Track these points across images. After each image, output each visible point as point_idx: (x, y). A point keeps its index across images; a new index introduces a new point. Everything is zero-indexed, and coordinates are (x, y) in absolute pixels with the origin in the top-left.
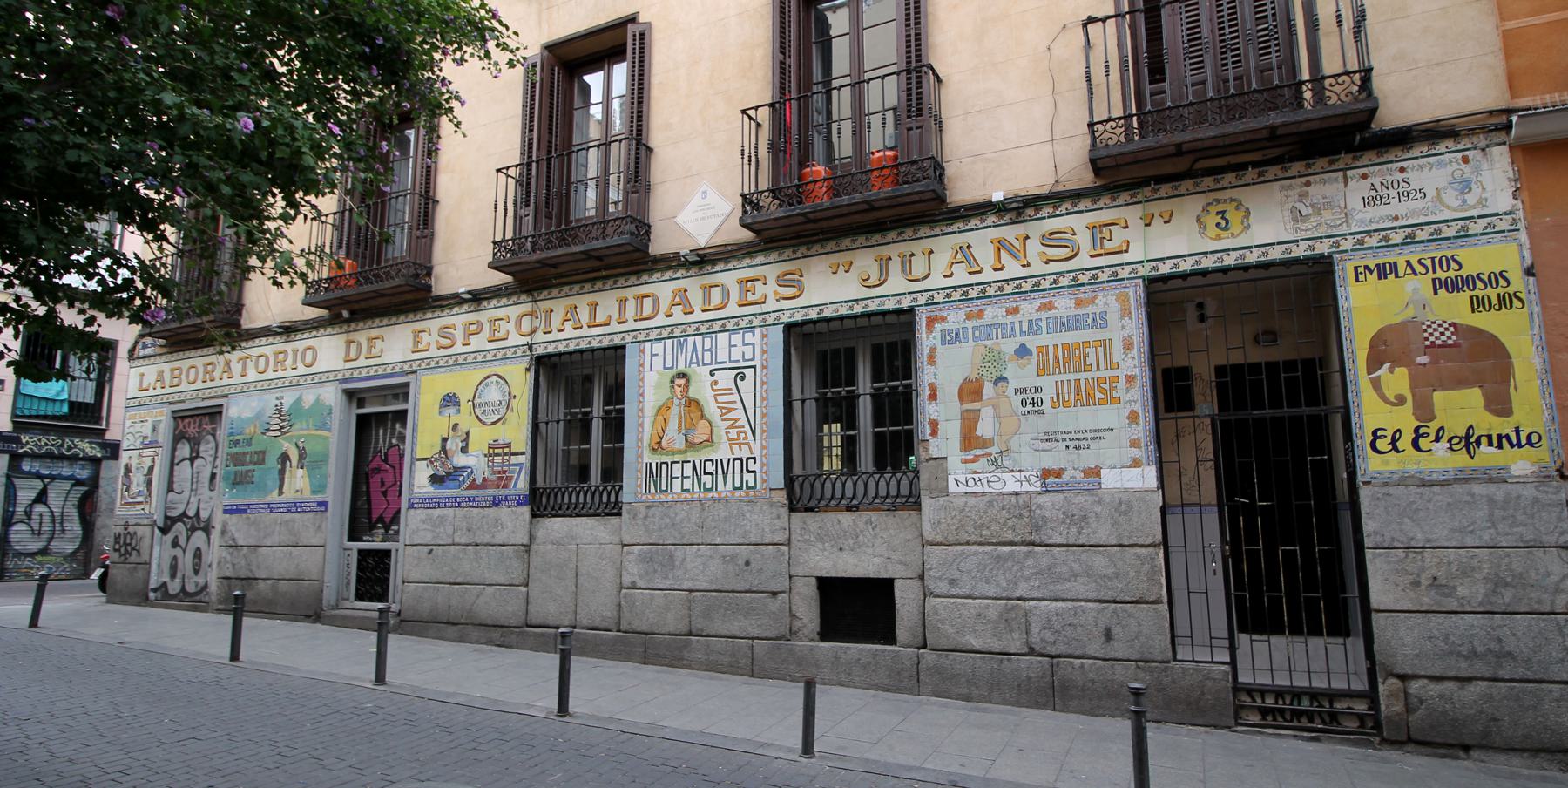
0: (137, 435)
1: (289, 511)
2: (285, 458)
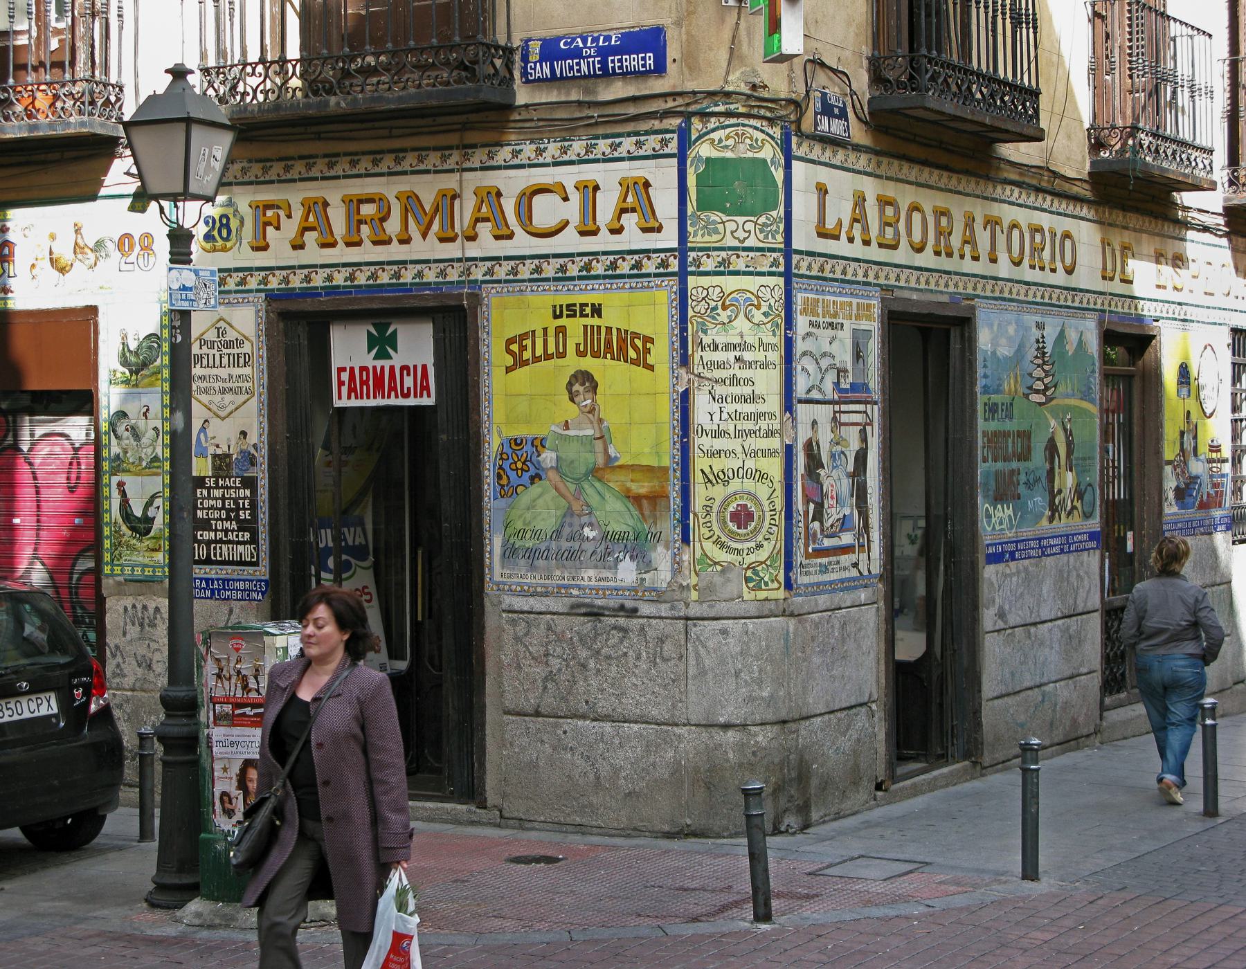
0: (825, 363)
1: (1062, 551)
2: (1052, 448)
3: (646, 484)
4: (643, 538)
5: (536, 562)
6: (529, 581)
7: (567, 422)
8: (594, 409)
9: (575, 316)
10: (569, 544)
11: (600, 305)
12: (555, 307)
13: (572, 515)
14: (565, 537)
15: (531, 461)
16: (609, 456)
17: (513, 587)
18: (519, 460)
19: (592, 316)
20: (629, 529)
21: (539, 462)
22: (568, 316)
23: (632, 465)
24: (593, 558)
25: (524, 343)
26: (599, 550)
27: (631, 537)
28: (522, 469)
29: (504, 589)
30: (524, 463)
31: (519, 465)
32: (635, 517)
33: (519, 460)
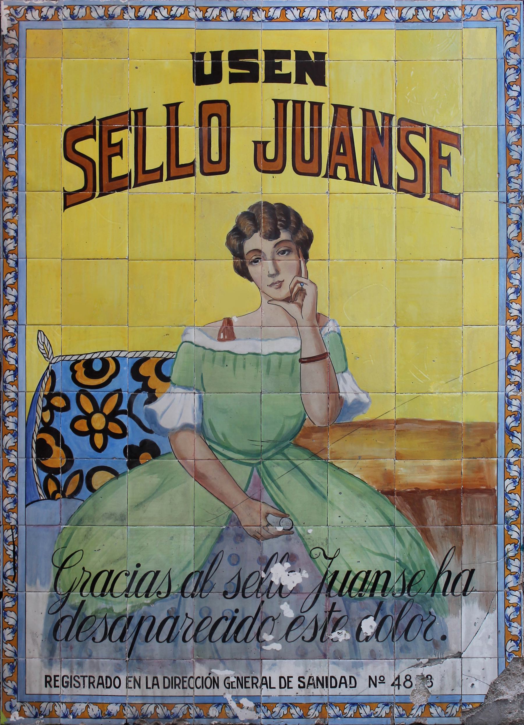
3: (435, 463)
4: (426, 584)
5: (141, 648)
6: (122, 691)
7: (229, 322)
8: (302, 292)
9: (253, 78)
10: (231, 604)
11: (320, 56)
12: (199, 56)
13: (239, 537)
14: (220, 587)
15: (129, 413)
16: (341, 401)
17: (80, 708)
18: (97, 409)
19: (301, 80)
20: (391, 566)
21: (152, 416)
22: (234, 79)
23: (398, 422)
24: (292, 635)
25: (116, 138)
26: (309, 616)
27: (395, 583)
28: (106, 432)
29: (52, 714)
30: (111, 418)
31: (98, 422)
32: (407, 539)
33: (97, 409)
